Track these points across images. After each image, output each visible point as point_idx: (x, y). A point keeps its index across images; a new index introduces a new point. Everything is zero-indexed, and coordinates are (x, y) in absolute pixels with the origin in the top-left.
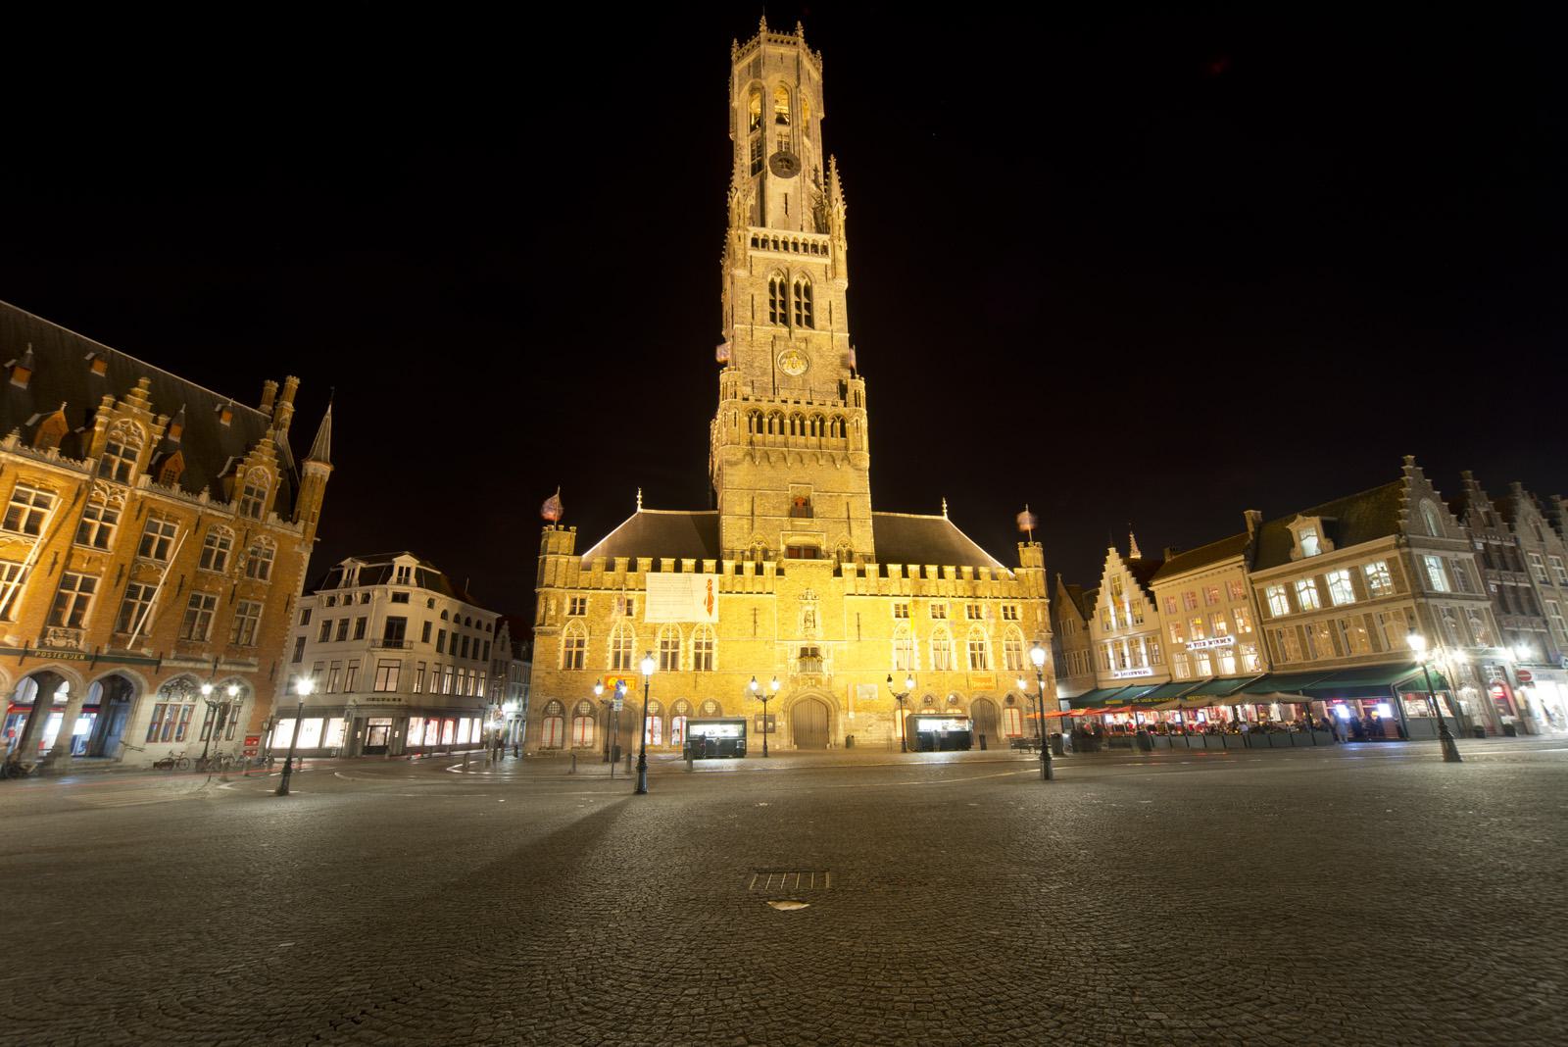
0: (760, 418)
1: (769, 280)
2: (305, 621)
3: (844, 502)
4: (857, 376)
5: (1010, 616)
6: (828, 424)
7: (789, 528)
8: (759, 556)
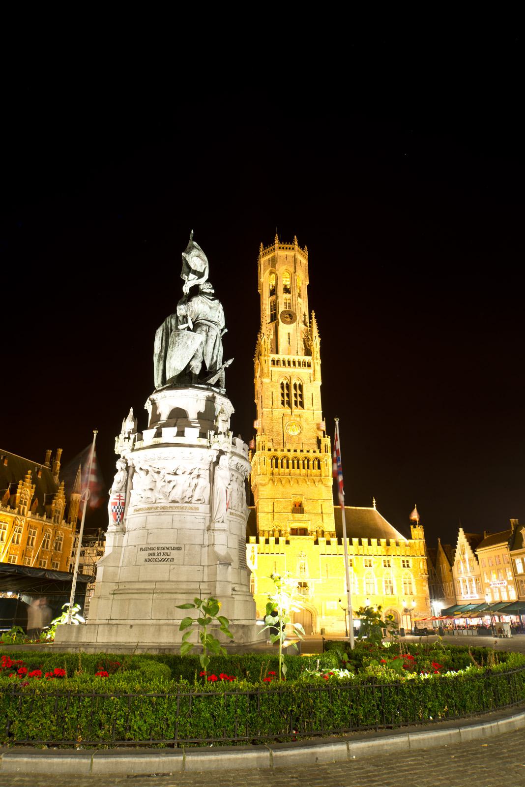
0: (277, 459)
1: (281, 383)
3: (320, 505)
4: (326, 436)
5: (406, 566)
6: (311, 463)
7: (292, 519)
8: (277, 534)
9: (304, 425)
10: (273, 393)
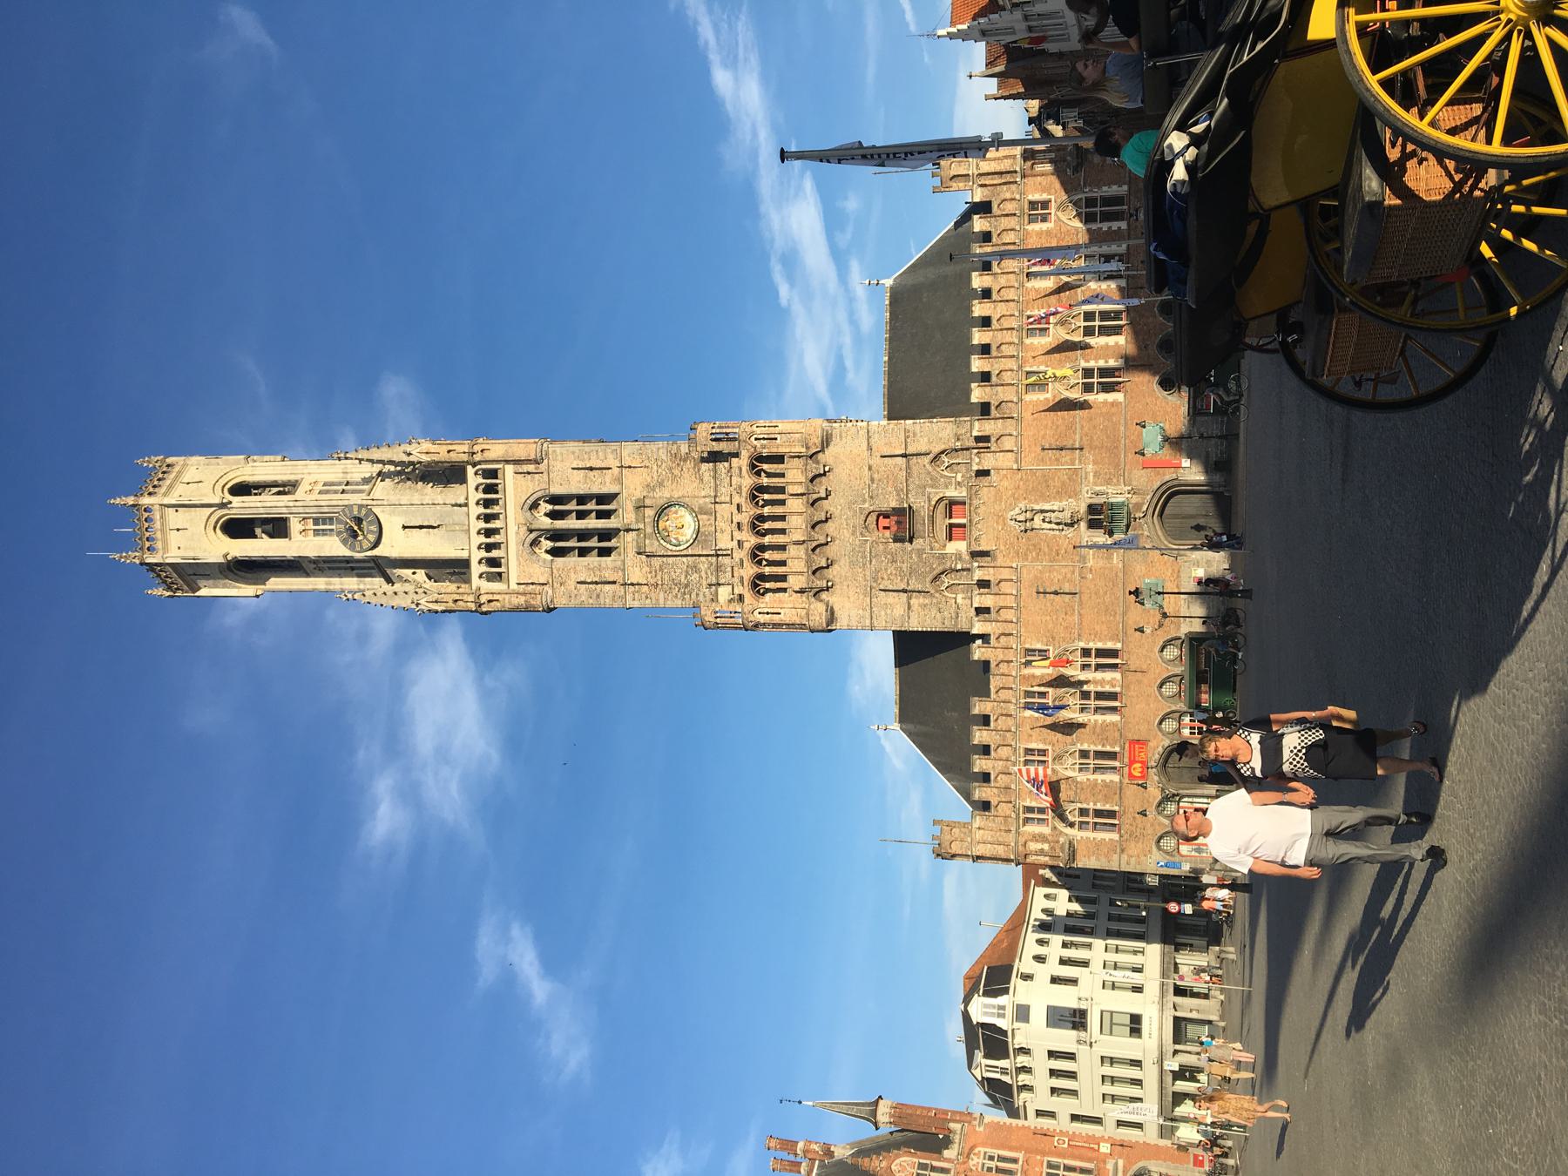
1: (549, 557)
2: (1052, 1115)
6: (765, 481)
9: (663, 495)
10: (582, 579)
